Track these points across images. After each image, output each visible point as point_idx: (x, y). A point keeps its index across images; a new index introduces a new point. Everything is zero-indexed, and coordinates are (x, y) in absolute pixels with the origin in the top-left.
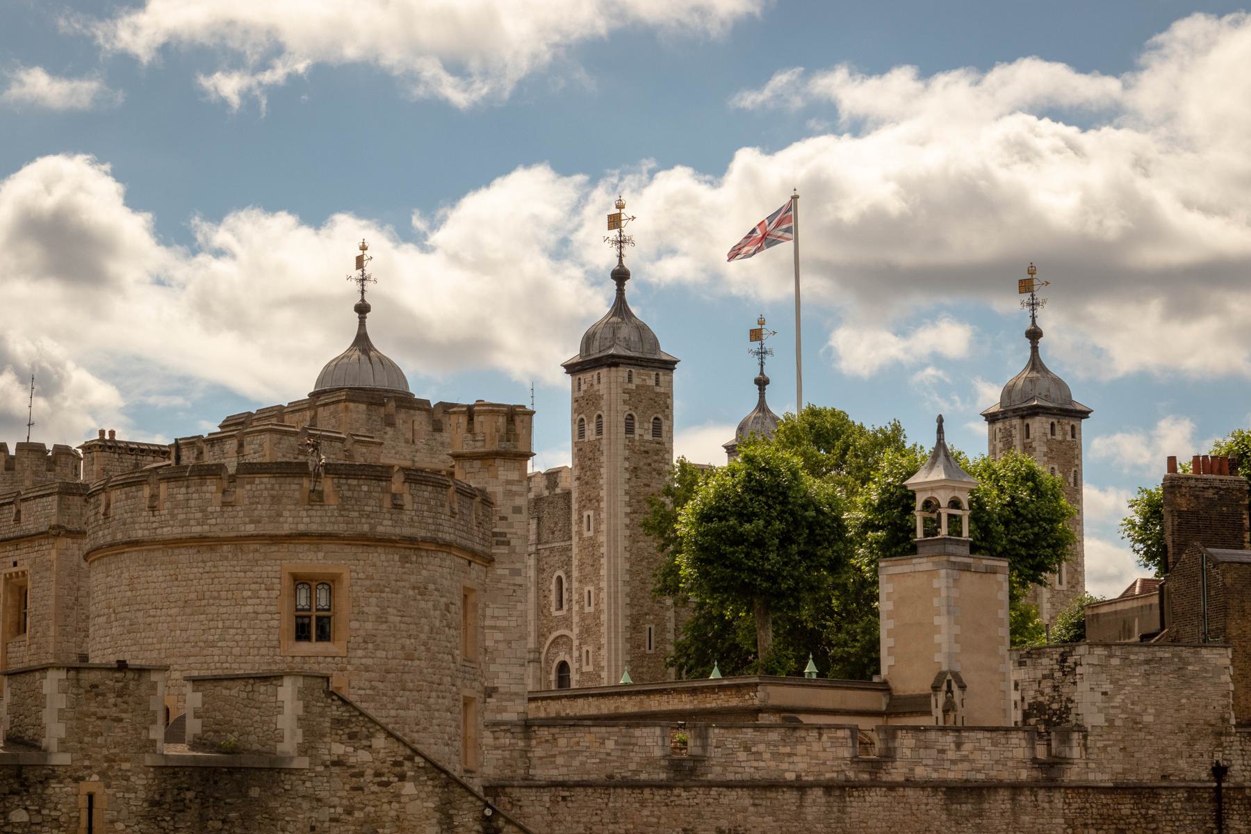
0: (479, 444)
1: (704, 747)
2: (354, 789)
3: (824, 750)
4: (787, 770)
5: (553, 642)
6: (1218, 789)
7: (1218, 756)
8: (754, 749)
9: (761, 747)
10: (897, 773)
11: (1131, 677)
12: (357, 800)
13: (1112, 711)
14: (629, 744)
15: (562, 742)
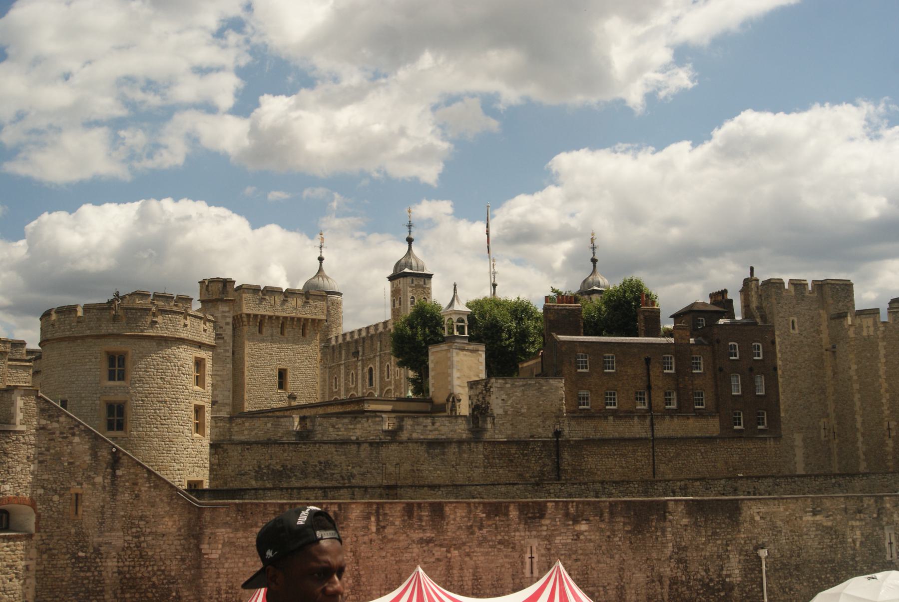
0: (210, 296)
1: (313, 426)
2: (50, 440)
3: (370, 426)
4: (352, 436)
5: (386, 392)
6: (557, 441)
7: (557, 427)
8: (337, 427)
9: (340, 426)
10: (404, 436)
11: (516, 392)
12: (52, 445)
13: (506, 407)
14: (278, 425)
15: (247, 424)
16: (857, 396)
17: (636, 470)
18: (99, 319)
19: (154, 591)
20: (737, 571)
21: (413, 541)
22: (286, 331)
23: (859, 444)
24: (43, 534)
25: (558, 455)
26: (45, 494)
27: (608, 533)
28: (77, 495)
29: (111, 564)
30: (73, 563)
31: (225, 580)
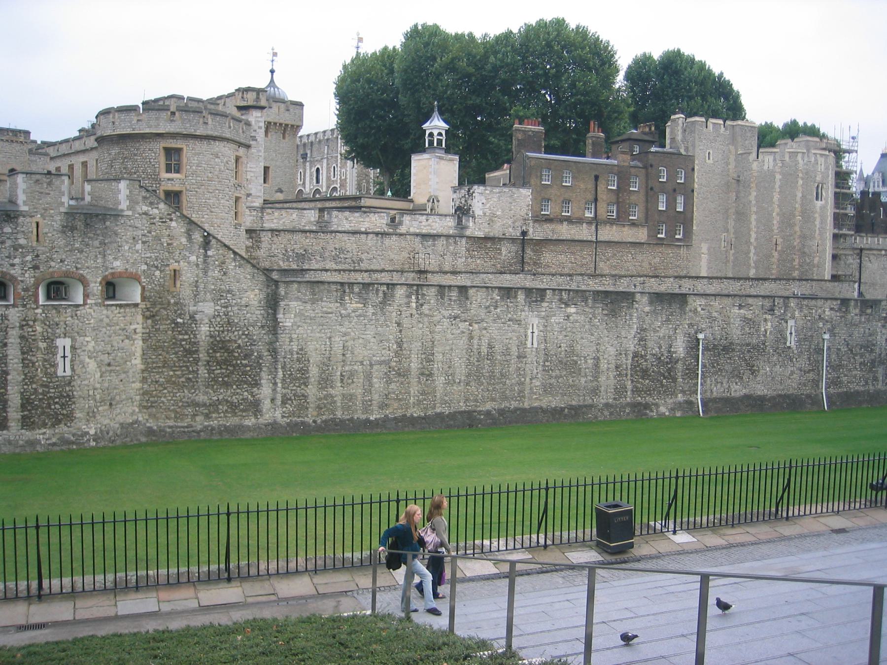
1: (331, 217)
7: (524, 228)
10: (403, 229)
15: (276, 214)
16: (754, 217)
17: (582, 266)
18: (157, 119)
19: (239, 351)
20: (681, 349)
21: (444, 317)
22: (269, 134)
23: (751, 255)
24: (148, 303)
25: (523, 251)
26: (149, 269)
27: (591, 316)
28: (175, 271)
29: (204, 329)
30: (173, 328)
31: (296, 343)
